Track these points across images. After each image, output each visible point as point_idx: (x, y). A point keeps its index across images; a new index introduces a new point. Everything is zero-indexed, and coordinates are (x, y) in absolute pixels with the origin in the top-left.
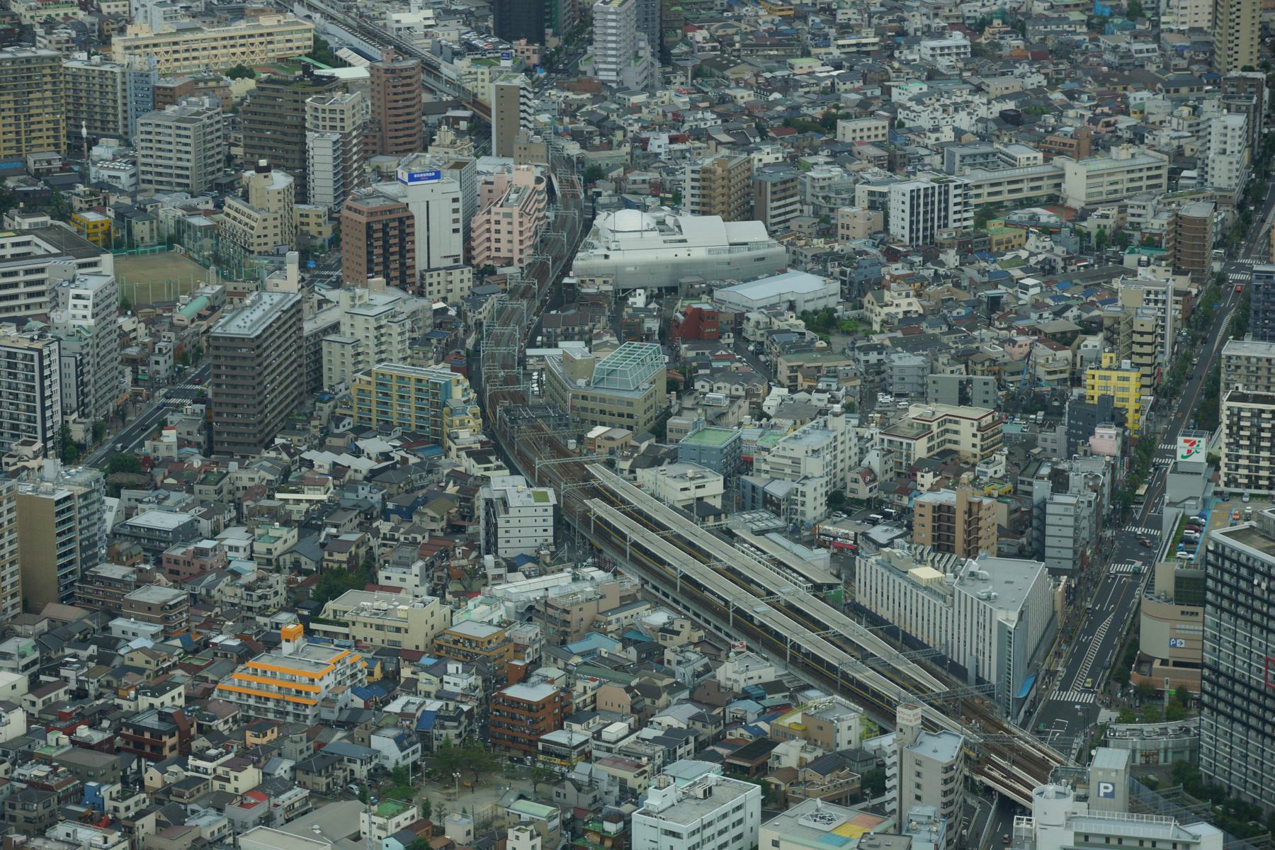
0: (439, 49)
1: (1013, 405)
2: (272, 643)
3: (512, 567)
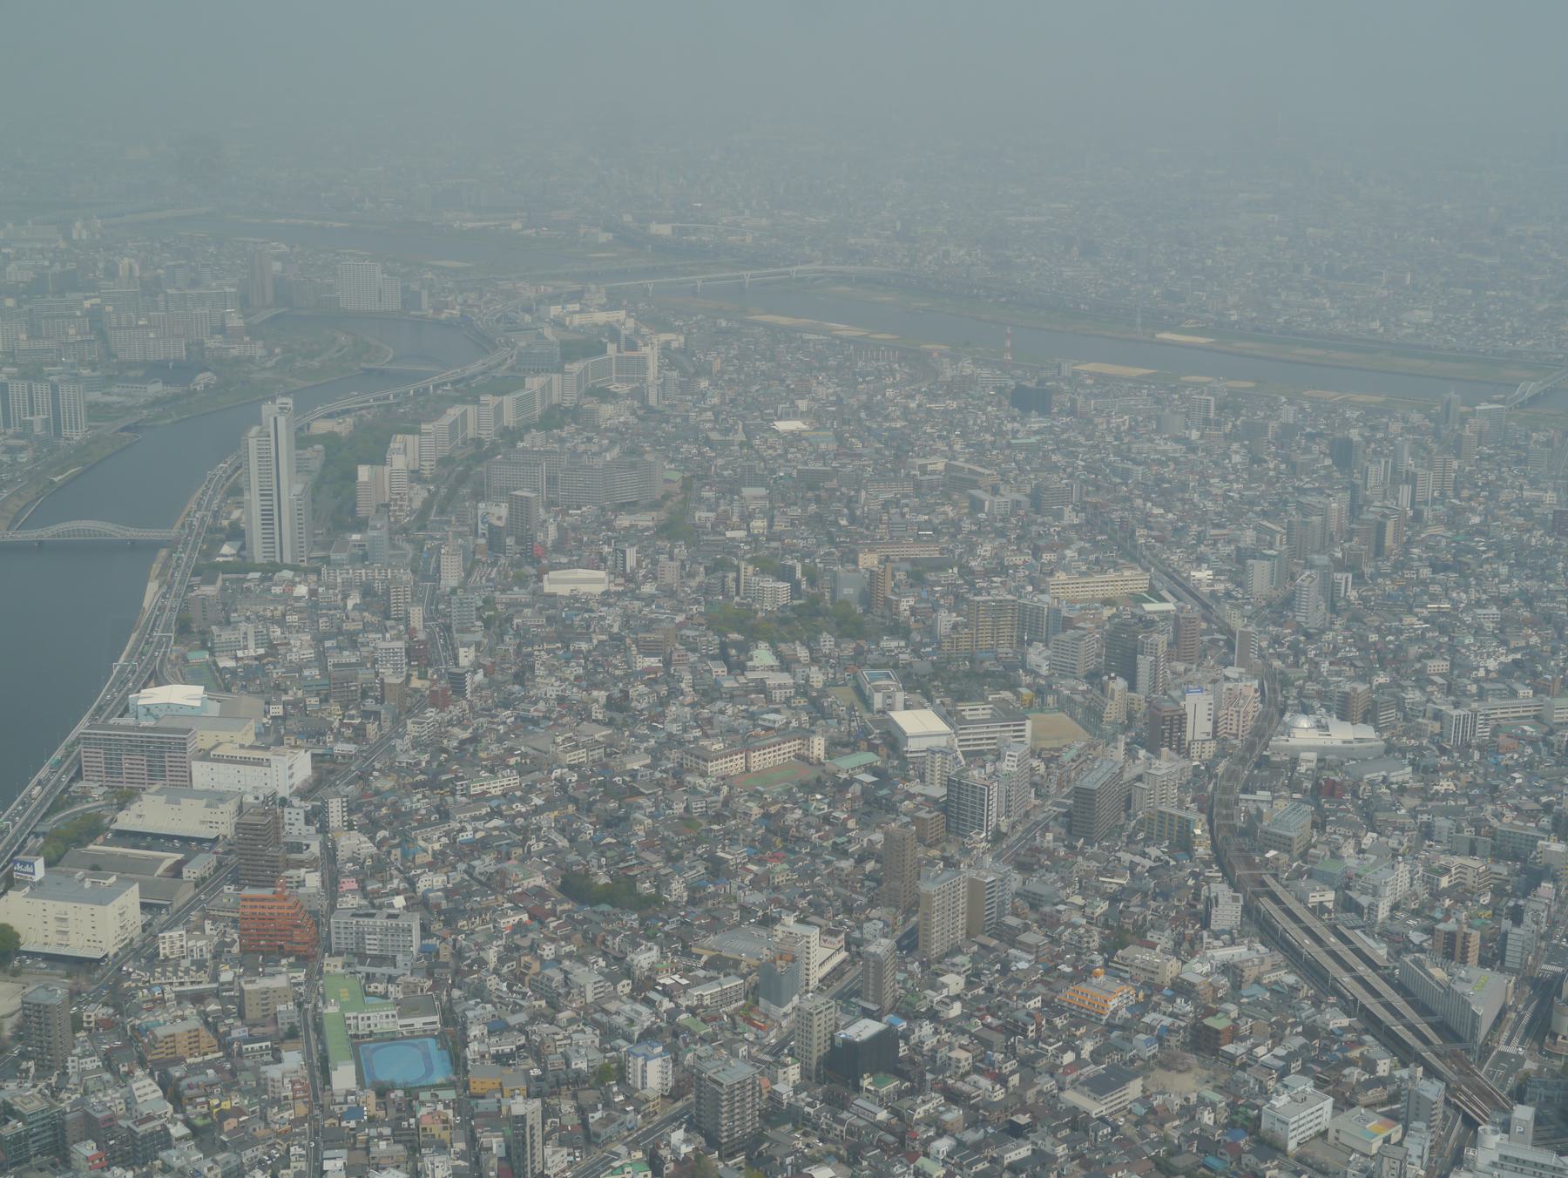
0: (1213, 594)
1: (1498, 854)
2: (1089, 972)
3: (1216, 936)
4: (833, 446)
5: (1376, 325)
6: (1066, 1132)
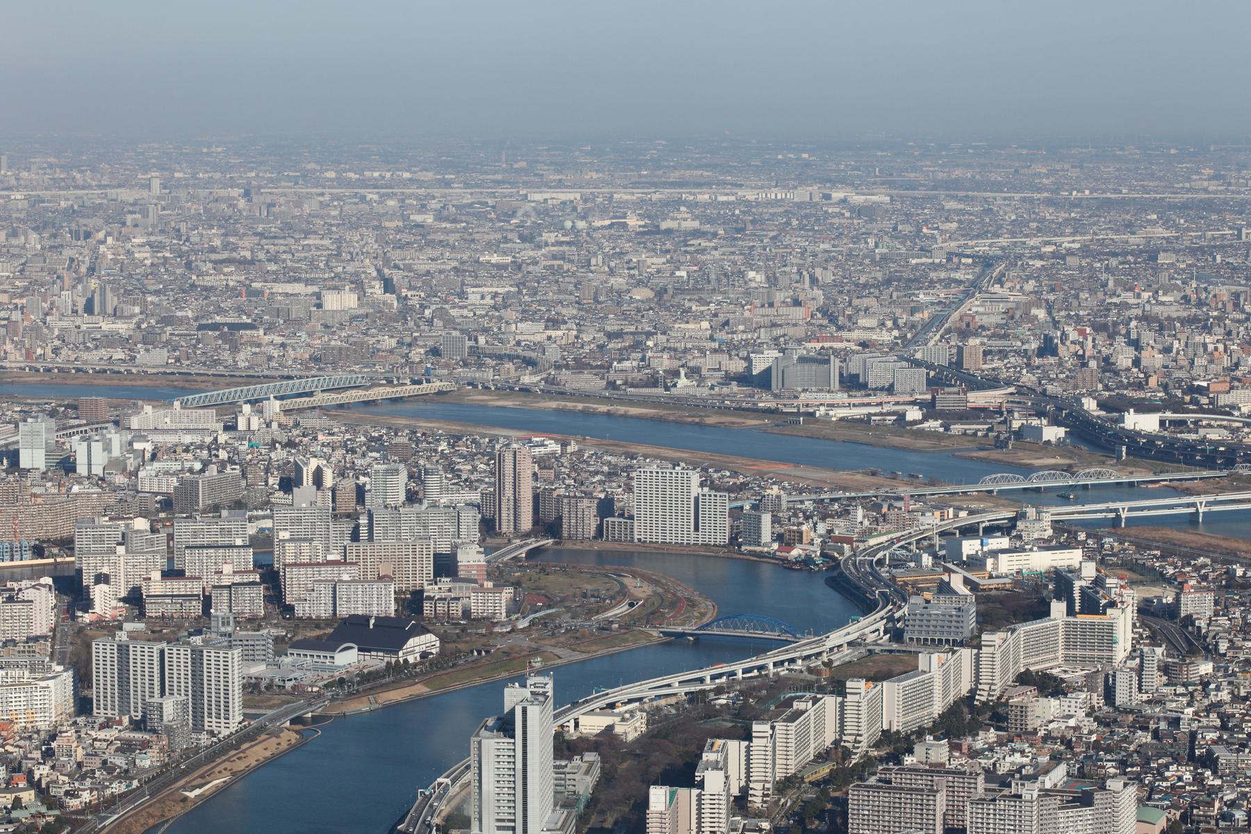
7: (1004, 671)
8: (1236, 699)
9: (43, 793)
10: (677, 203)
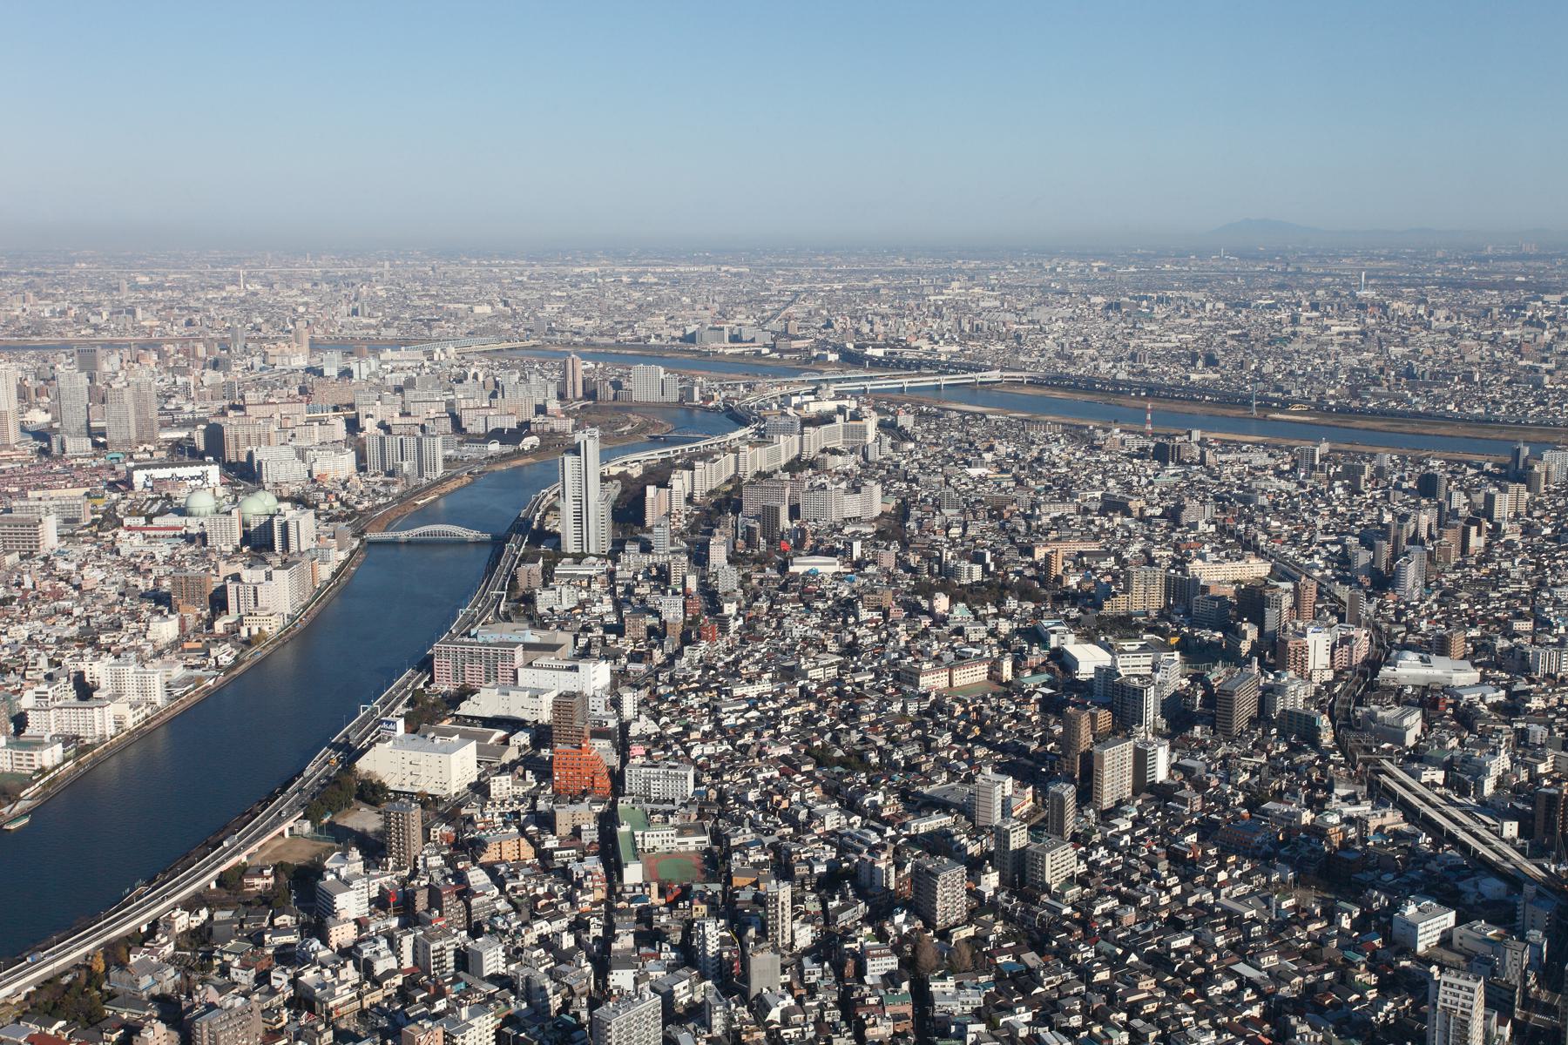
4: (1013, 484)
5: (1451, 407)
6: (1223, 927)
7: (815, 446)
8: (925, 457)
9: (343, 503)
10: (646, 273)
